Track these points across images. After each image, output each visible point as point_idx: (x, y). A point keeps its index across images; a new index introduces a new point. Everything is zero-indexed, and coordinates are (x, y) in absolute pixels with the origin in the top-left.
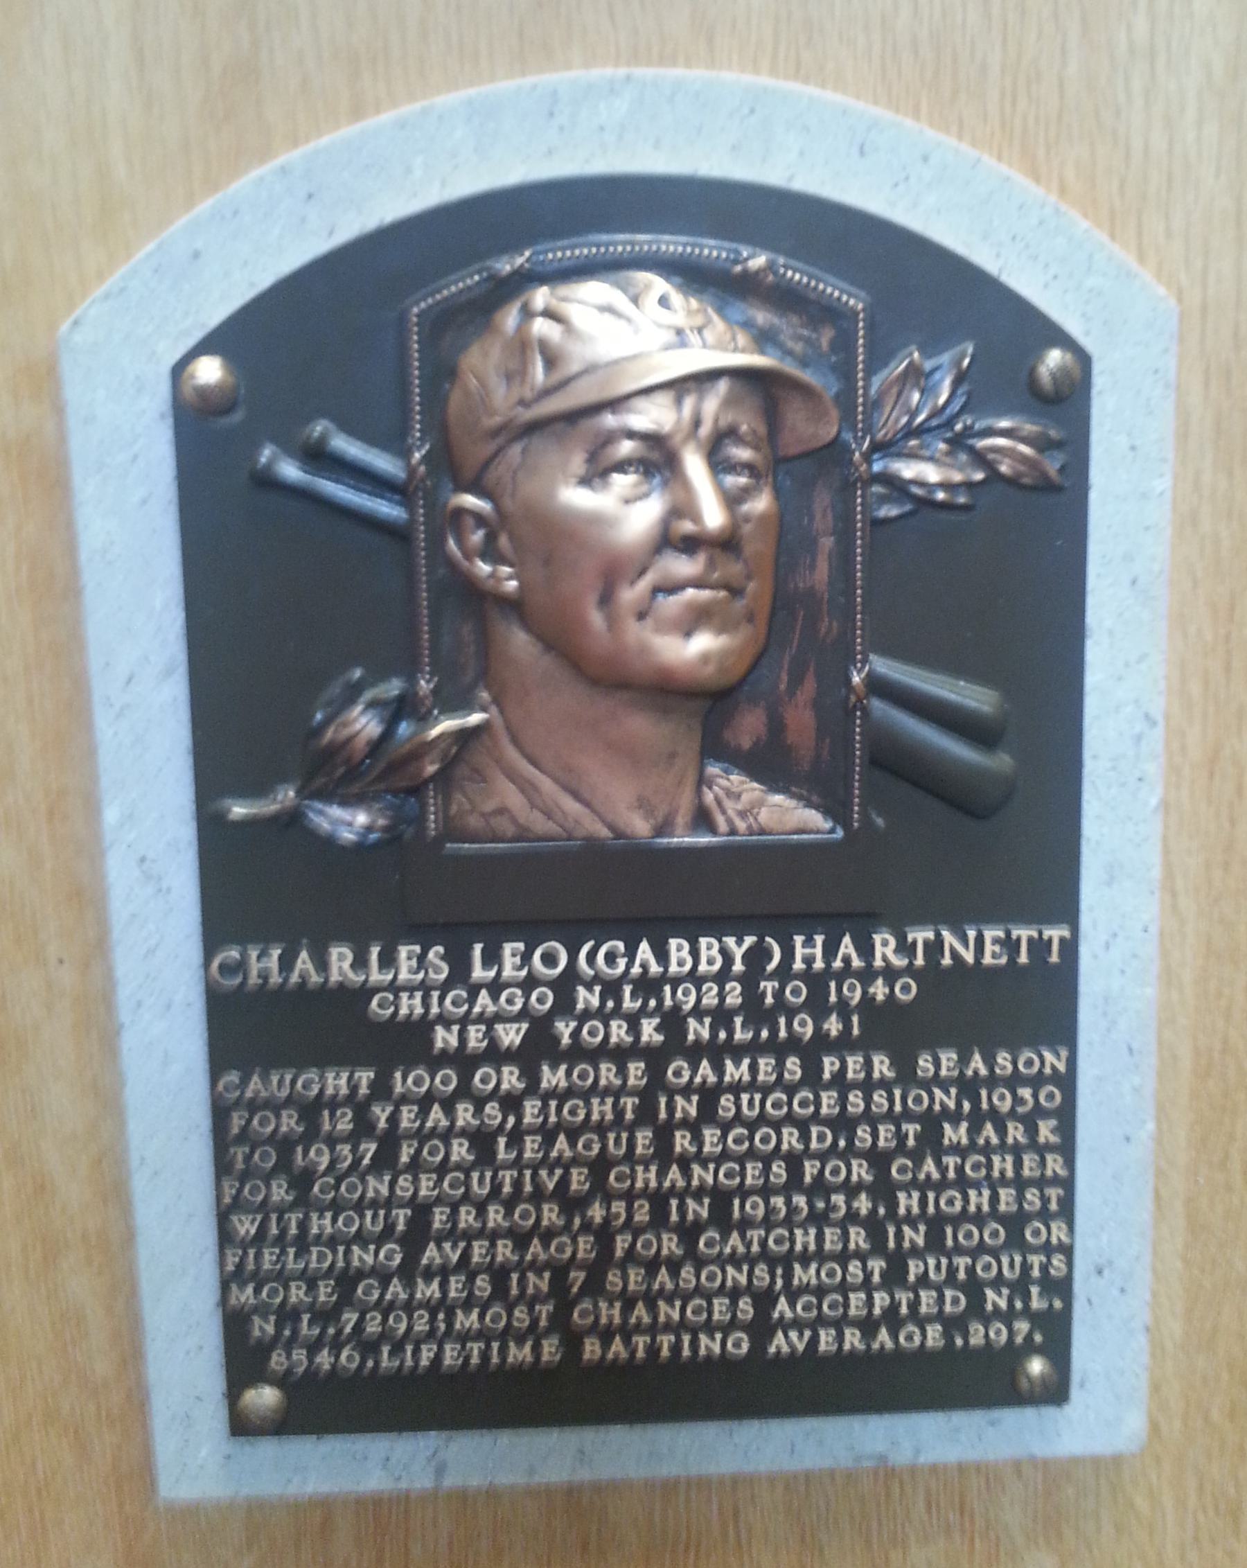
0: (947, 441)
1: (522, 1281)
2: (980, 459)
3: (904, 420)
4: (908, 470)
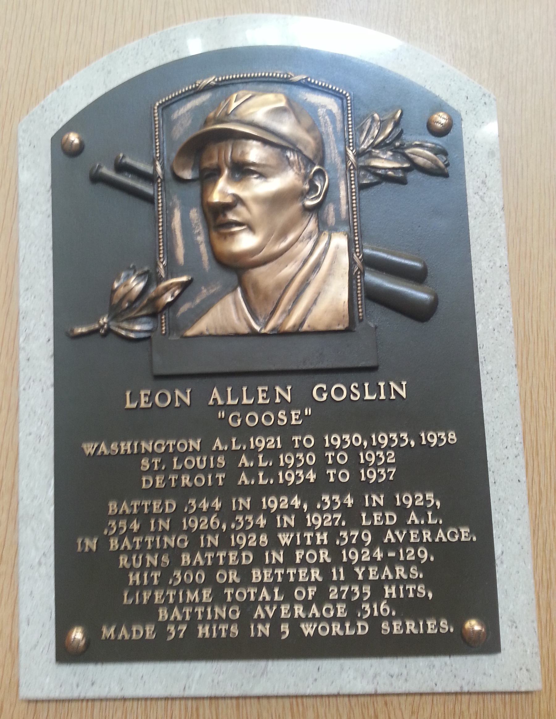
0: (391, 150)
1: (156, 524)
3: (371, 141)
4: (376, 163)
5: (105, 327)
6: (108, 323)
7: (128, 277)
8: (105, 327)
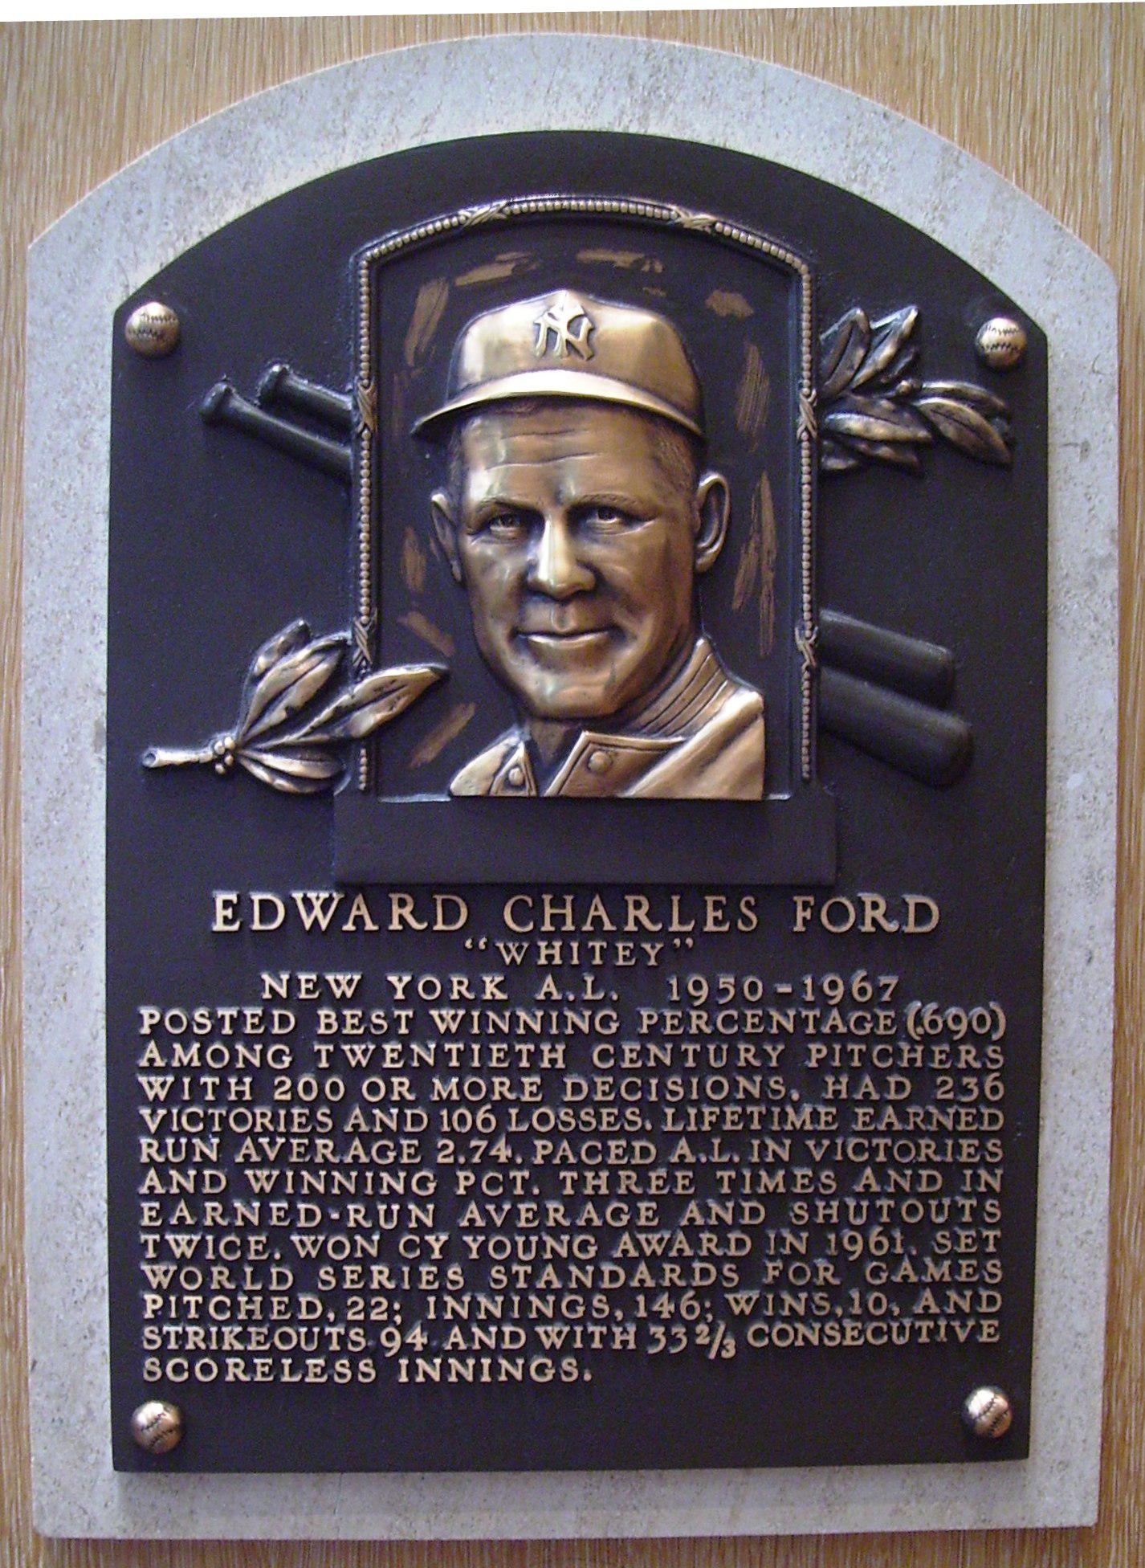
0: (889, 399)
2: (923, 419)
3: (850, 373)
4: (854, 423)
5: (228, 759)
6: (234, 751)
7: (286, 650)
8: (228, 759)
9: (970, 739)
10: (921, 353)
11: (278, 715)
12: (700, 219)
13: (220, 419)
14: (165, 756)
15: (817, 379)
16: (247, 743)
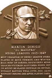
2: (45, 17)
9: (48, 36)
10: (45, 13)
11: (8, 35)
12: (32, 5)
13: (5, 18)
14: (1, 37)
15: (39, 14)
16: (6, 36)
